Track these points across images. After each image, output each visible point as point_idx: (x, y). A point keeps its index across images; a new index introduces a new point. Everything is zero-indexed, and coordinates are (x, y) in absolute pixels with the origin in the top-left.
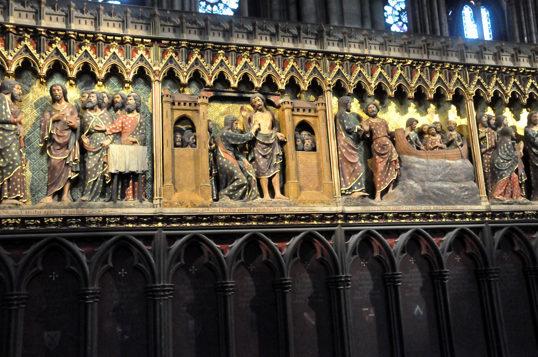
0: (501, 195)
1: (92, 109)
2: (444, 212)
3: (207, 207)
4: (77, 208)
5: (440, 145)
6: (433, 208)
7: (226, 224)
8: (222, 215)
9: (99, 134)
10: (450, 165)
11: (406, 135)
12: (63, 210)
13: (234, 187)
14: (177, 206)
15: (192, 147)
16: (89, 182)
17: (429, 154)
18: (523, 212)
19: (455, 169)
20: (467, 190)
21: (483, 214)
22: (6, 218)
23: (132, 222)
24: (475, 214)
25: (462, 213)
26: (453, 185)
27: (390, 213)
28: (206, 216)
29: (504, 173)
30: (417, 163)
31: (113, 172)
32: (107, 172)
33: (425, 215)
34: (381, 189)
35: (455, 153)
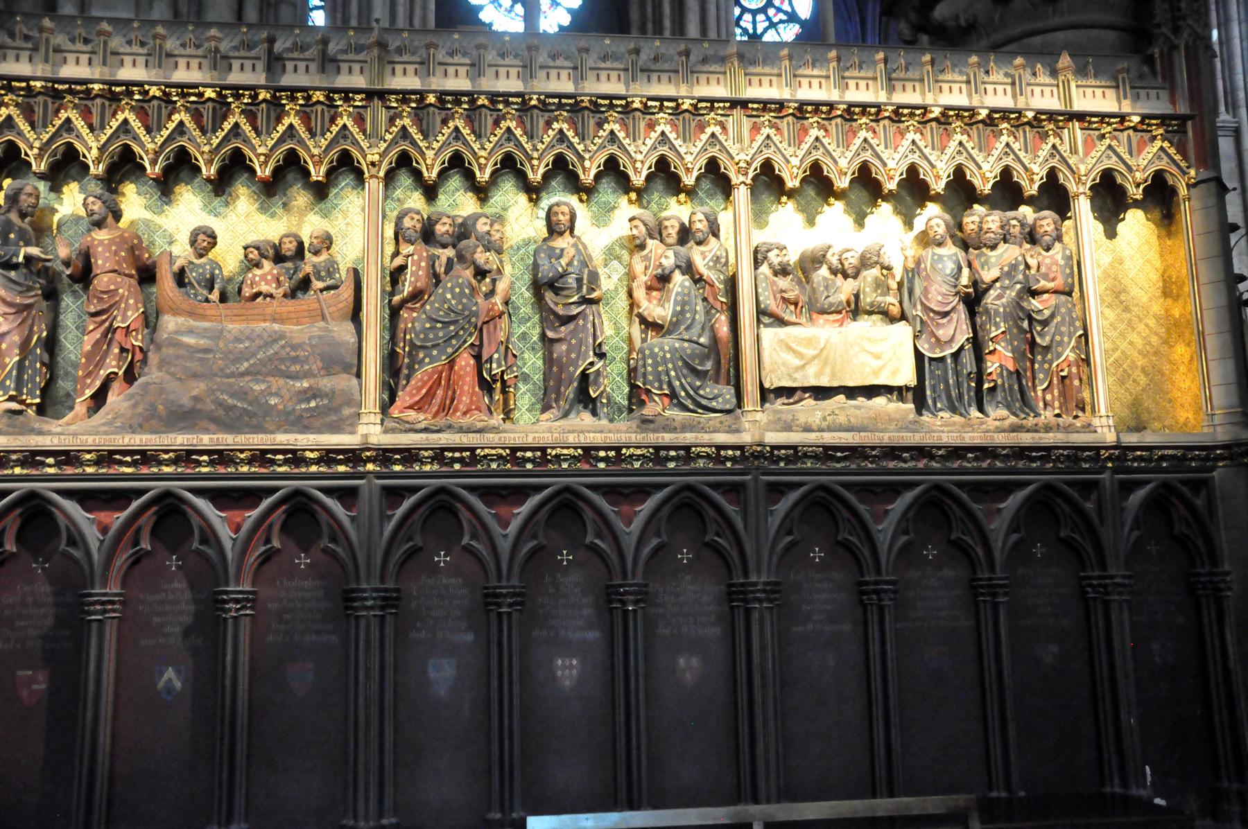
0: (411, 407)
2: (242, 451)
5: (264, 288)
6: (206, 440)
10: (282, 336)
11: (176, 268)
17: (228, 312)
18: (472, 450)
19: (294, 347)
20: (314, 397)
21: (353, 456)
24: (328, 457)
25: (294, 452)
26: (277, 383)
27: (89, 452)
29: (431, 356)
30: (190, 331)
33: (186, 456)
34: (83, 394)
35: (305, 307)
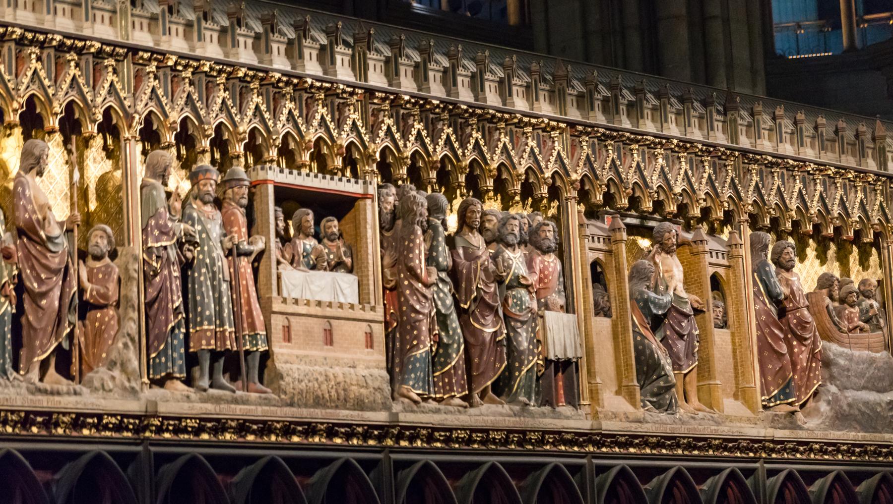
1: (508, 245)
3: (640, 422)
4: (520, 416)
7: (654, 452)
8: (652, 436)
9: (523, 291)
12: (507, 418)
13: (660, 388)
14: (611, 419)
15: (605, 316)
16: (523, 373)
22: (456, 429)
23: (566, 442)
28: (636, 437)
31: (552, 357)
32: (541, 357)
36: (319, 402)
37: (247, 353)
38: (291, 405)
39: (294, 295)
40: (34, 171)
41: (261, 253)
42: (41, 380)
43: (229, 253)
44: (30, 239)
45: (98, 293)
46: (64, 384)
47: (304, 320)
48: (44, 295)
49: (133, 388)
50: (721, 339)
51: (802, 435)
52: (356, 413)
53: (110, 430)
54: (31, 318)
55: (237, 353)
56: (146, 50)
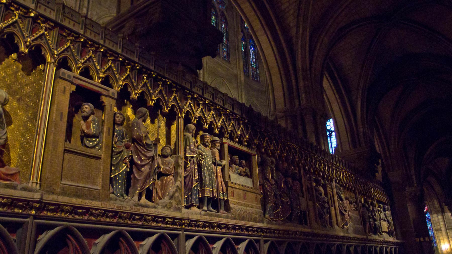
36: (243, 219)
37: (220, 199)
38: (235, 219)
39: (234, 182)
40: (142, 119)
41: (224, 166)
42: (139, 200)
43: (215, 164)
44: (138, 143)
45: (166, 169)
46: (149, 203)
47: (238, 190)
48: (143, 166)
49: (179, 208)
50: (333, 209)
51: (350, 235)
52: (254, 223)
53: (169, 224)
54: (136, 175)
55: (217, 199)
56: (188, 90)
